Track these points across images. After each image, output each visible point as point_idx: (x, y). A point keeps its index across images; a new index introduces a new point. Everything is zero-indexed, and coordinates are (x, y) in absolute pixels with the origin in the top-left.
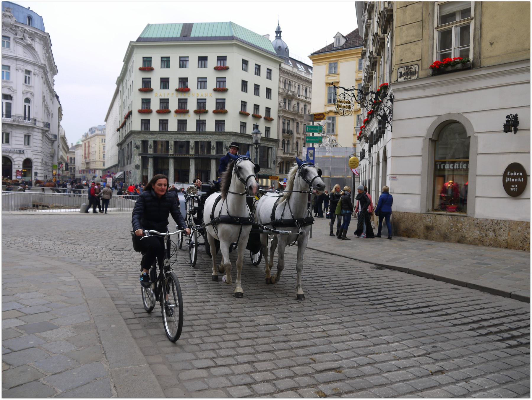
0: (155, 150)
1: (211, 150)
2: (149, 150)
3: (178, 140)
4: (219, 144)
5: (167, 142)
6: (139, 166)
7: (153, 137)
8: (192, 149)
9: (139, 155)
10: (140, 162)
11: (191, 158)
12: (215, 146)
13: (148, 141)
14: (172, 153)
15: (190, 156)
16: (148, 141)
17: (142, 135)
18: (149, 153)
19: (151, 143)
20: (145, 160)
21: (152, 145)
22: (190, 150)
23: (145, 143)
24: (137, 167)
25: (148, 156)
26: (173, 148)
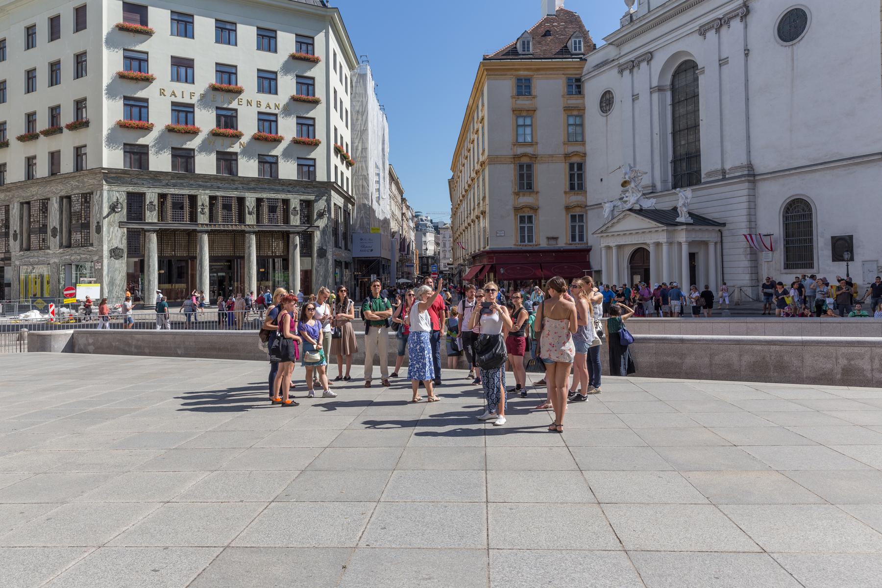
0: (162, 216)
1: (292, 217)
2: (148, 213)
4: (307, 205)
8: (250, 213)
9: (121, 224)
10: (125, 242)
11: (249, 232)
12: (298, 209)
15: (247, 229)
16: (142, 195)
18: (148, 220)
21: (156, 202)
22: (247, 216)
24: (115, 253)
25: (146, 227)
26: (207, 210)
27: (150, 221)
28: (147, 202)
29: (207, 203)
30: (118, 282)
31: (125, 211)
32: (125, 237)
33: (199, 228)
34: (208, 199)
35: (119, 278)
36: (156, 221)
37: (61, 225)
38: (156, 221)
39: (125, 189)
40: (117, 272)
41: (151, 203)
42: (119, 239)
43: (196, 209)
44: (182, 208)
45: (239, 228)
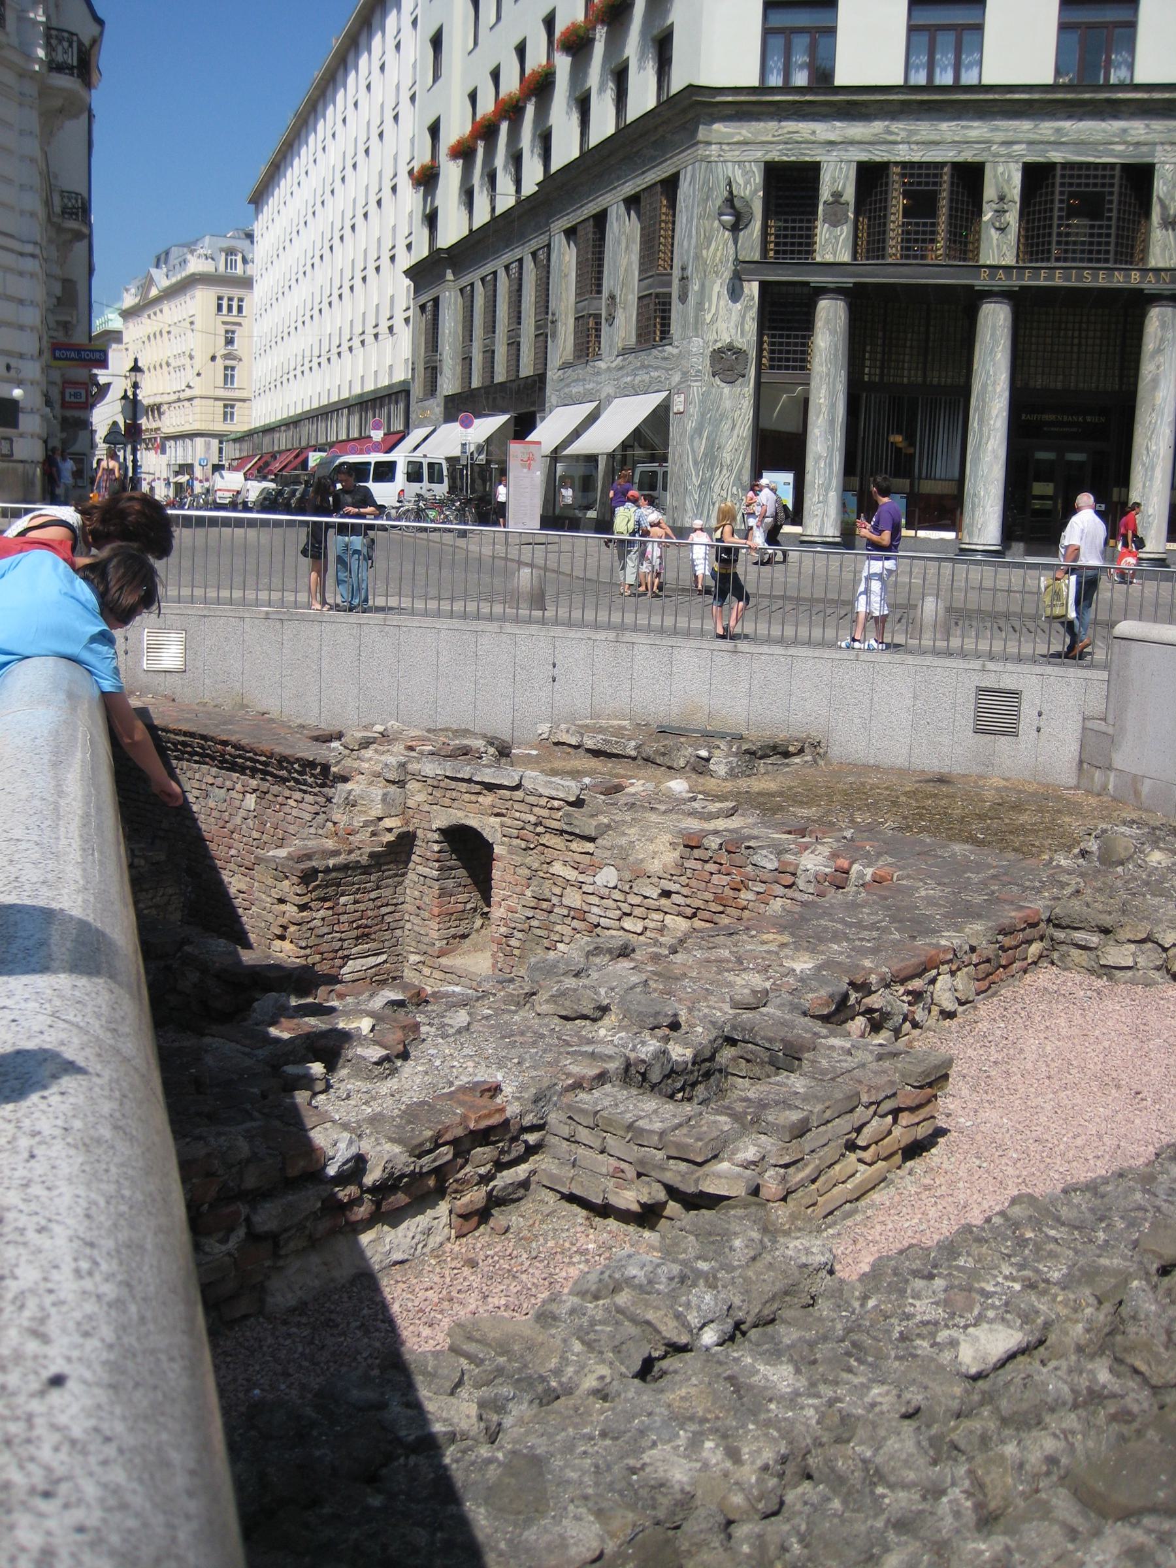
3: (1056, 156)
5: (970, 176)
6: (739, 352)
7: (857, 130)
10: (751, 326)
11: (1155, 298)
13: (815, 167)
14: (1010, 260)
15: (1150, 284)
16: (815, 167)
19: (837, 180)
20: (785, 316)
21: (849, 195)
23: (791, 187)
24: (725, 362)
25: (815, 280)
26: (1012, 217)
27: (829, 258)
28: (825, 194)
29: (1015, 192)
30: (727, 456)
33: (982, 281)
34: (1017, 178)
35: (731, 444)
36: (846, 257)
38: (846, 257)
39: (759, 154)
40: (726, 426)
41: (837, 195)
43: (979, 213)
44: (932, 212)
45: (1118, 280)
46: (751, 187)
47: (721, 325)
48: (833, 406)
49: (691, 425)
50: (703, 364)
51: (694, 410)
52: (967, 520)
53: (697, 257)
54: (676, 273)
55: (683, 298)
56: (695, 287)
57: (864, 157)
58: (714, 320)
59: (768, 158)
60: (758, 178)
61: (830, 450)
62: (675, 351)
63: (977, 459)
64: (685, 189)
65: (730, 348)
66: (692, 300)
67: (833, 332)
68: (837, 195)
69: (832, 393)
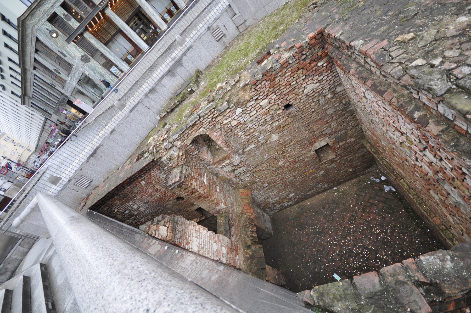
6: (84, 55)
9: (68, 41)
10: (80, 50)
17: (38, 12)
18: (76, 27)
24: (85, 59)
27: (76, 27)
28: (63, 17)
30: (103, 73)
31: (59, 32)
32: (78, 48)
36: (79, 24)
37: (54, 66)
38: (79, 24)
39: (44, 20)
40: (97, 69)
41: (64, 14)
42: (76, 51)
46: (50, 26)
47: (76, 54)
48: (106, 50)
49: (93, 74)
50: (82, 63)
51: (90, 71)
52: (141, 48)
53: (58, 47)
54: (59, 54)
55: (65, 56)
56: (65, 52)
57: (60, 4)
58: (74, 55)
59: (46, 19)
60: (49, 24)
61: (114, 57)
62: (75, 66)
63: (133, 38)
64: (41, 38)
65: (82, 56)
66: (67, 55)
67: (92, 38)
68: (64, 14)
69: (104, 48)
